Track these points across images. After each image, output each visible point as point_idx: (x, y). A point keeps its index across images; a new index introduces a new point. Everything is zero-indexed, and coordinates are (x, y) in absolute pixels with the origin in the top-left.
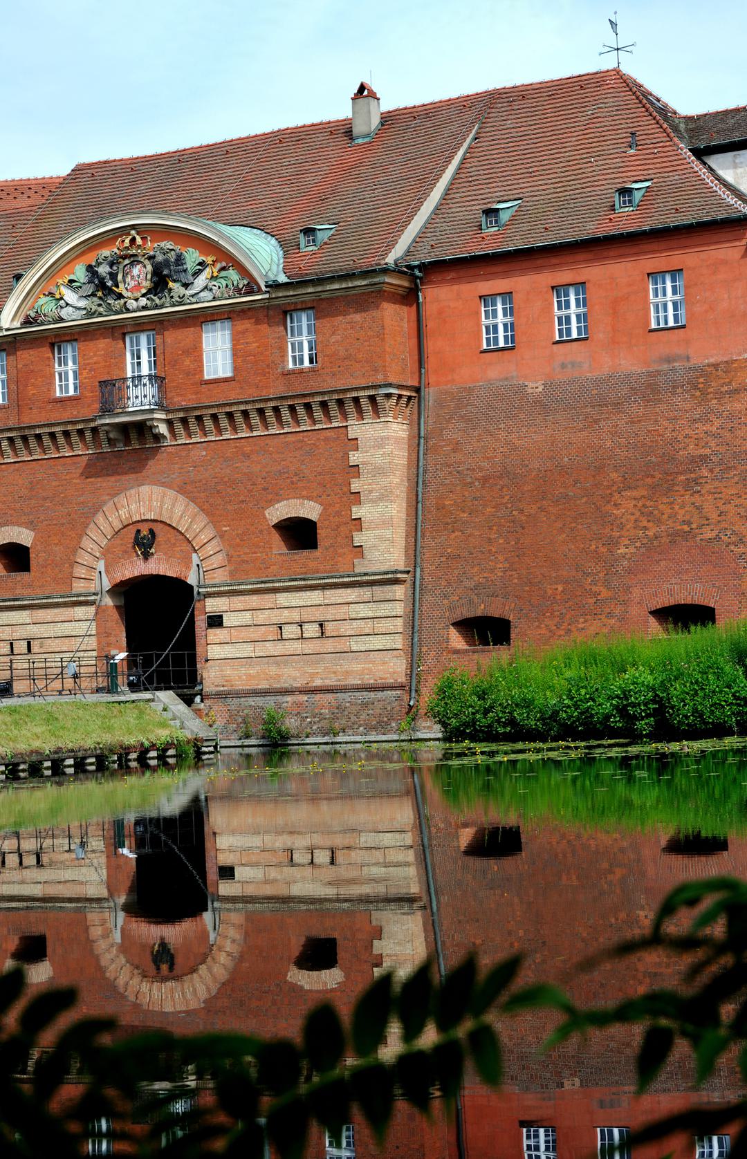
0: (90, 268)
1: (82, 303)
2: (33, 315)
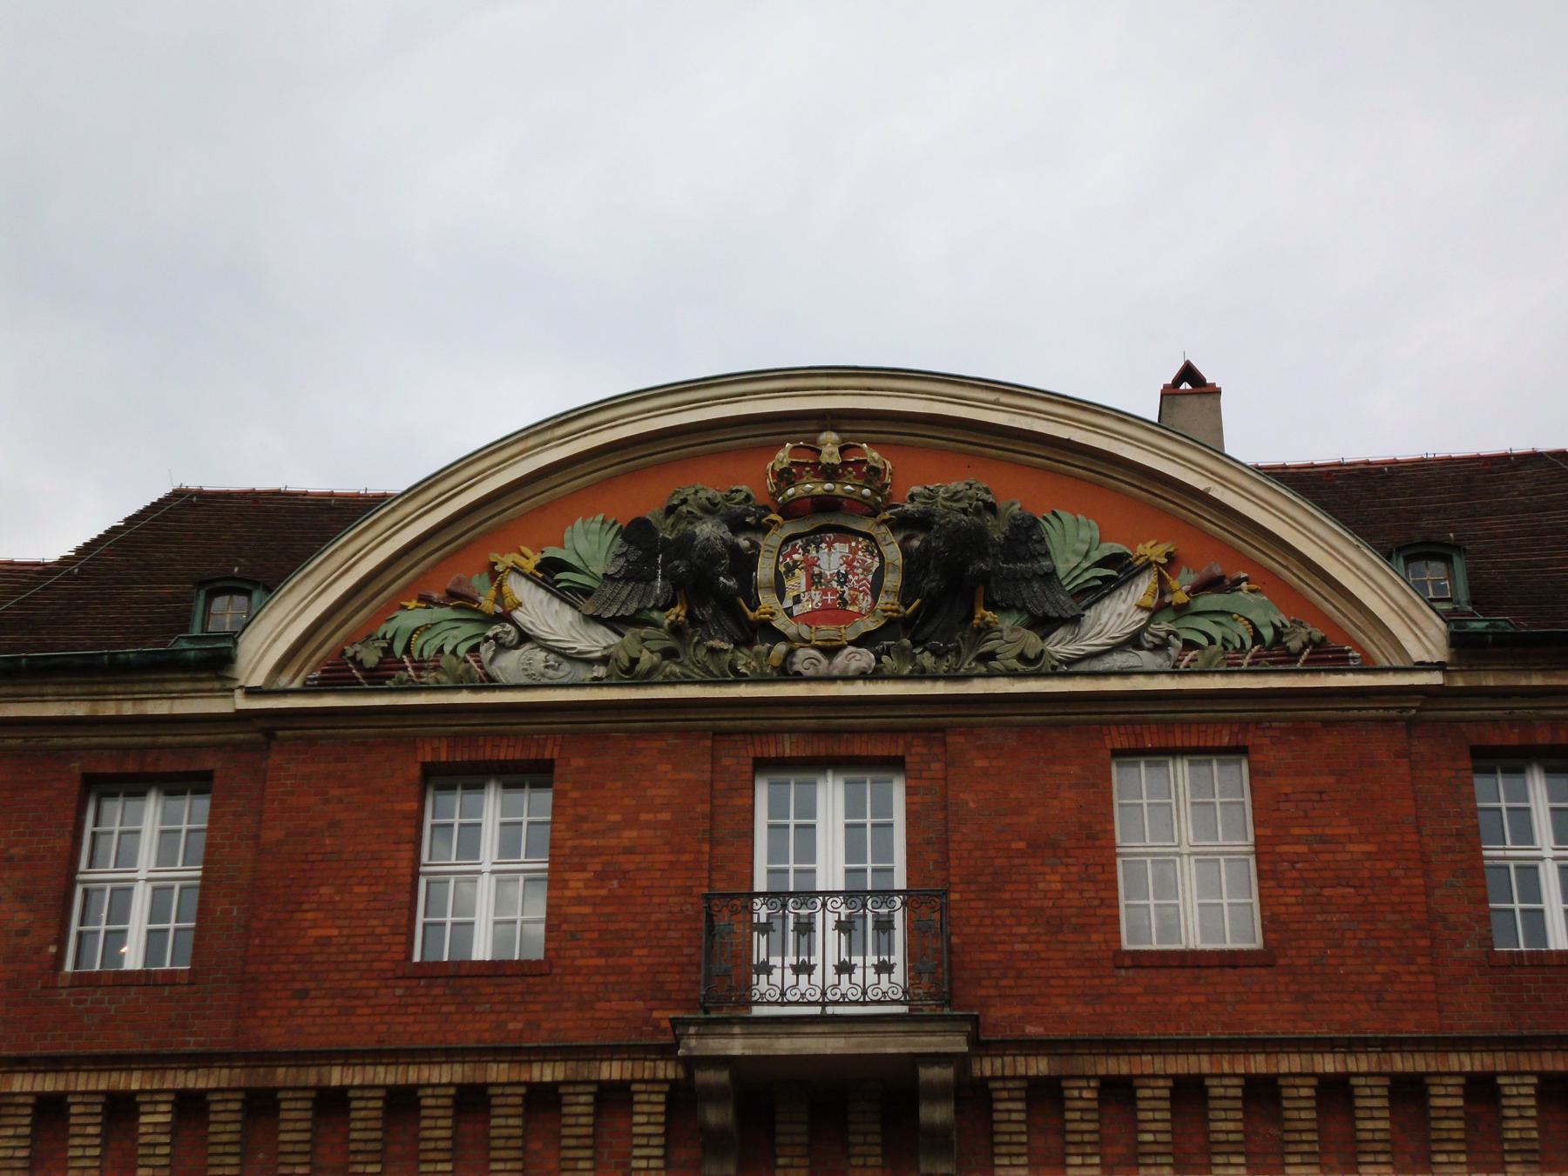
0: (637, 533)
1: (596, 640)
2: (371, 657)
